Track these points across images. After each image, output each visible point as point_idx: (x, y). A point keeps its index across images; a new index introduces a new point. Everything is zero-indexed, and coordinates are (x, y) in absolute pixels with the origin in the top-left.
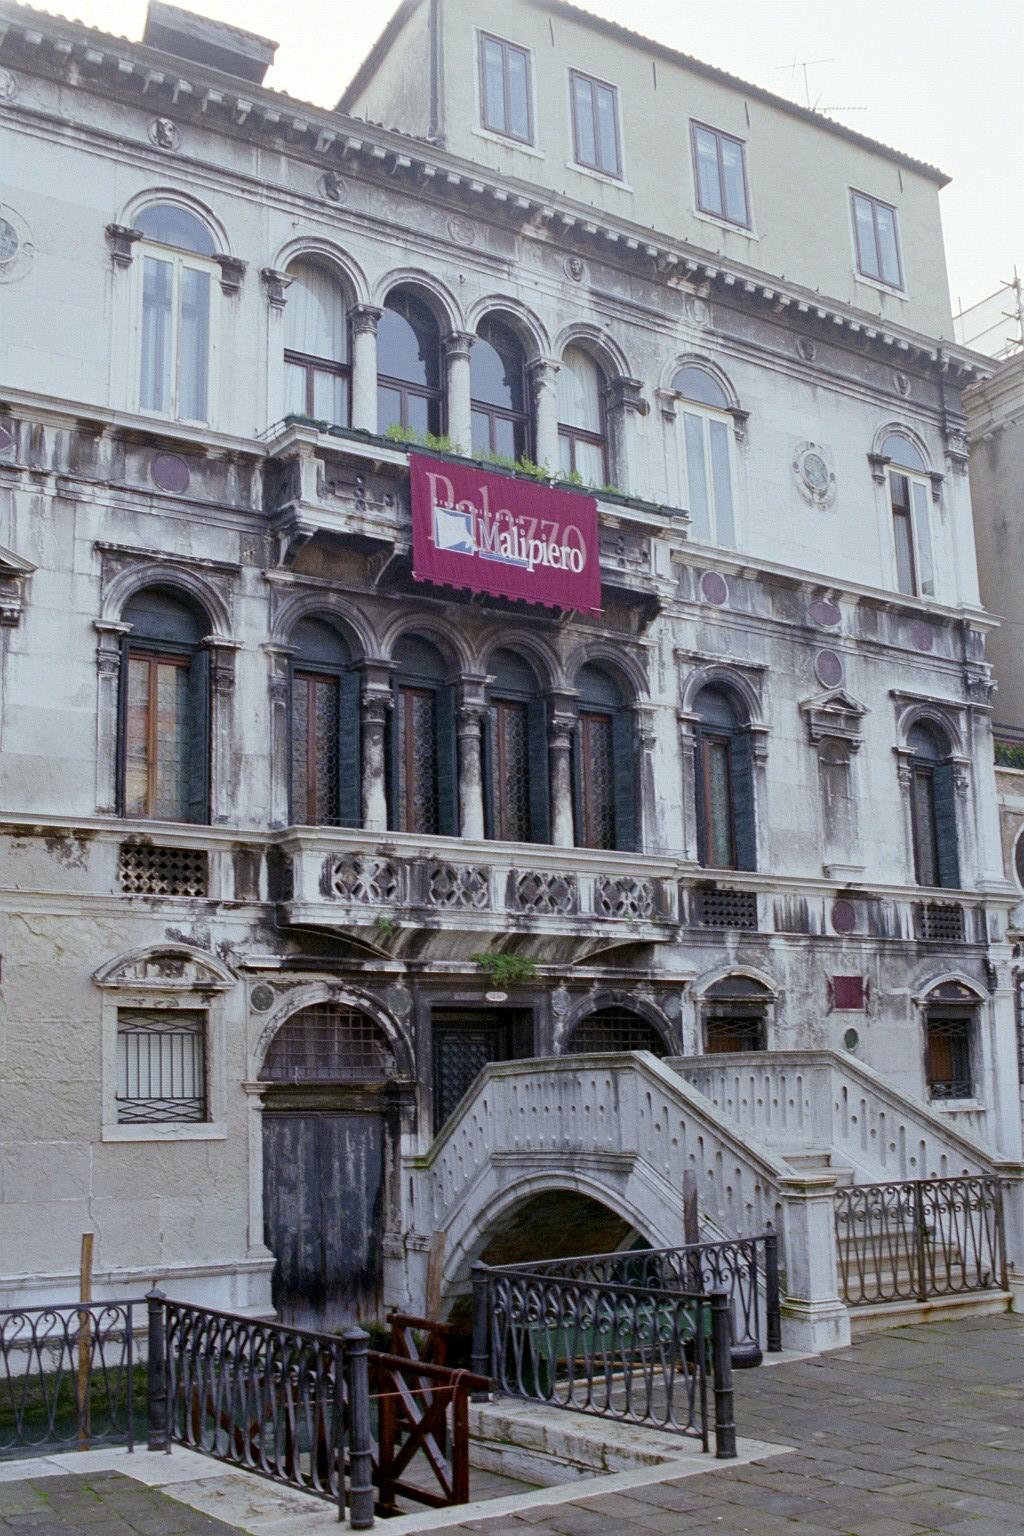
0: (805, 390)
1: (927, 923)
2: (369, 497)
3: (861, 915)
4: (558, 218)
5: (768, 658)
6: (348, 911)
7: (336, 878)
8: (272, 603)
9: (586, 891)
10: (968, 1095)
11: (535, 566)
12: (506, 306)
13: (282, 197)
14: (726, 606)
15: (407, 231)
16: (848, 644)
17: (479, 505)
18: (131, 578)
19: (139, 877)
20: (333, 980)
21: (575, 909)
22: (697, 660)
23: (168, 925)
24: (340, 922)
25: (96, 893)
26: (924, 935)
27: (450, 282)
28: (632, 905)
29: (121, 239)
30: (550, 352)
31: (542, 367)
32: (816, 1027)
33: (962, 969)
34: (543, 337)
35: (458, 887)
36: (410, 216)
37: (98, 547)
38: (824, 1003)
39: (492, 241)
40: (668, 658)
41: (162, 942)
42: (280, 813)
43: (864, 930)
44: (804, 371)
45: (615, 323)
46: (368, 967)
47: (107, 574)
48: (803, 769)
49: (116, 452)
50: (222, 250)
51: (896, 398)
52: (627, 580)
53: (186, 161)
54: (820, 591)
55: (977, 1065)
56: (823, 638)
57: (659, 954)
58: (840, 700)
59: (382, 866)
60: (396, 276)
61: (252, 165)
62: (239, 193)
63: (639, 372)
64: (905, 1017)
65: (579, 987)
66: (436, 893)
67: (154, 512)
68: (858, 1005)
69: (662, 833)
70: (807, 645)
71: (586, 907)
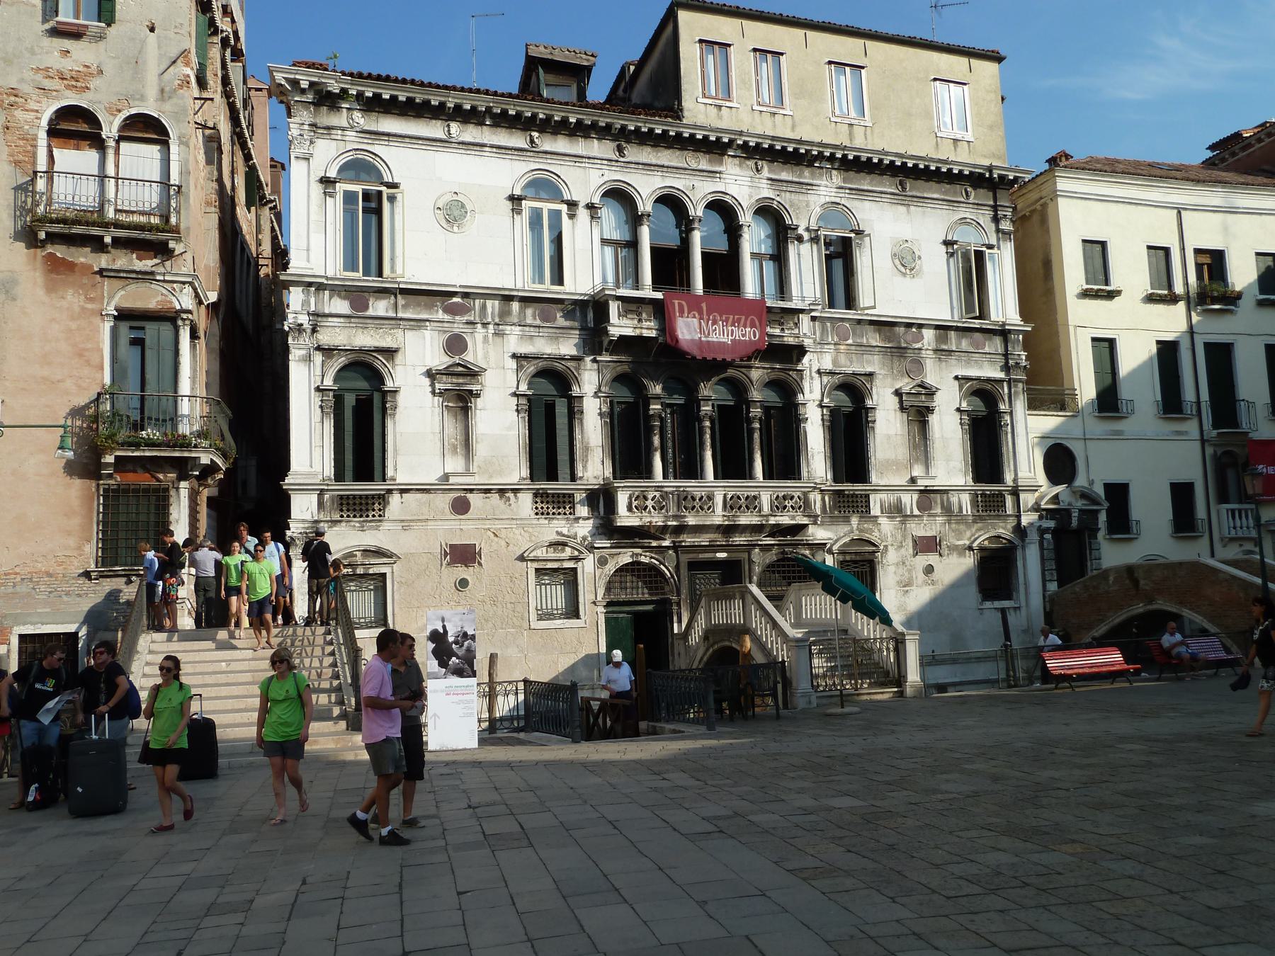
0: (902, 209)
1: (980, 504)
2: (644, 315)
3: (936, 502)
4: (746, 143)
5: (876, 367)
6: (641, 519)
9: (765, 500)
10: (1009, 598)
11: (731, 340)
12: (719, 196)
13: (596, 161)
14: (850, 341)
15: (663, 166)
16: (928, 352)
17: (701, 313)
18: (531, 368)
19: (542, 508)
20: (638, 551)
21: (760, 511)
22: (831, 373)
23: (556, 529)
24: (637, 524)
25: (523, 516)
26: (978, 511)
27: (687, 189)
28: (792, 506)
29: (515, 200)
30: (746, 218)
31: (742, 225)
32: (907, 563)
33: (1004, 528)
34: (741, 209)
36: (666, 157)
37: (514, 356)
38: (911, 551)
39: (710, 161)
41: (554, 537)
42: (608, 472)
43: (938, 510)
44: (903, 198)
45: (783, 194)
46: (654, 544)
48: (898, 425)
49: (521, 307)
50: (567, 196)
51: (963, 203)
52: (786, 339)
53: (546, 152)
55: (1014, 582)
57: (811, 529)
58: (922, 386)
59: (658, 496)
60: (658, 192)
62: (573, 164)
63: (797, 218)
64: (965, 557)
65: (766, 548)
66: (685, 508)
67: (541, 334)
71: (766, 509)
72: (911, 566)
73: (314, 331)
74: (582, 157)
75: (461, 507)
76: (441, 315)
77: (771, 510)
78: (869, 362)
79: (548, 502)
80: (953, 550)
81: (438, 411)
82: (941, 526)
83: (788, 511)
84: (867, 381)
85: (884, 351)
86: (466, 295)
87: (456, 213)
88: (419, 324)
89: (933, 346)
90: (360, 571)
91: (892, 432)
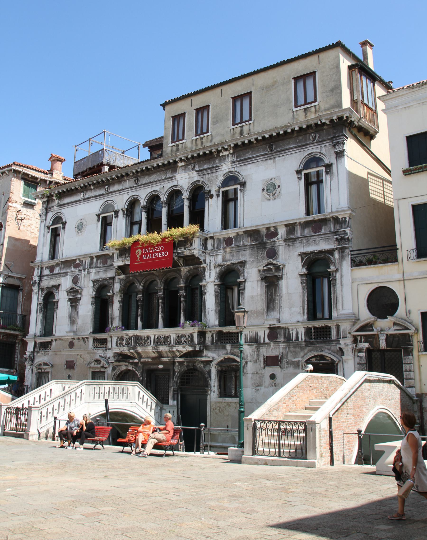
2: (127, 255)
3: (280, 334)
7: (118, 342)
8: (120, 282)
15: (151, 183)
20: (127, 364)
21: (169, 344)
22: (219, 265)
29: (98, 216)
33: (329, 350)
35: (143, 341)
36: (153, 178)
38: (262, 365)
39: (172, 172)
40: (212, 267)
41: (98, 357)
43: (282, 339)
46: (131, 361)
47: (94, 285)
48: (259, 289)
52: (185, 253)
54: (268, 229)
56: (269, 244)
57: (205, 353)
58: (272, 264)
60: (149, 195)
61: (122, 186)
64: (299, 369)
65: (181, 363)
66: (138, 344)
68: (277, 365)
69: (208, 318)
70: (264, 248)
71: (173, 342)
72: (261, 374)
73: (39, 284)
74: (121, 190)
75: (71, 345)
76: (73, 269)
77: (176, 344)
78: (243, 255)
79: (98, 343)
80: (291, 364)
81: (69, 307)
82: (283, 349)
83: (183, 344)
84: (241, 266)
85: (252, 247)
86: (79, 259)
87: (80, 227)
88: (66, 274)
89: (285, 237)
90: (43, 371)
91: (255, 294)
